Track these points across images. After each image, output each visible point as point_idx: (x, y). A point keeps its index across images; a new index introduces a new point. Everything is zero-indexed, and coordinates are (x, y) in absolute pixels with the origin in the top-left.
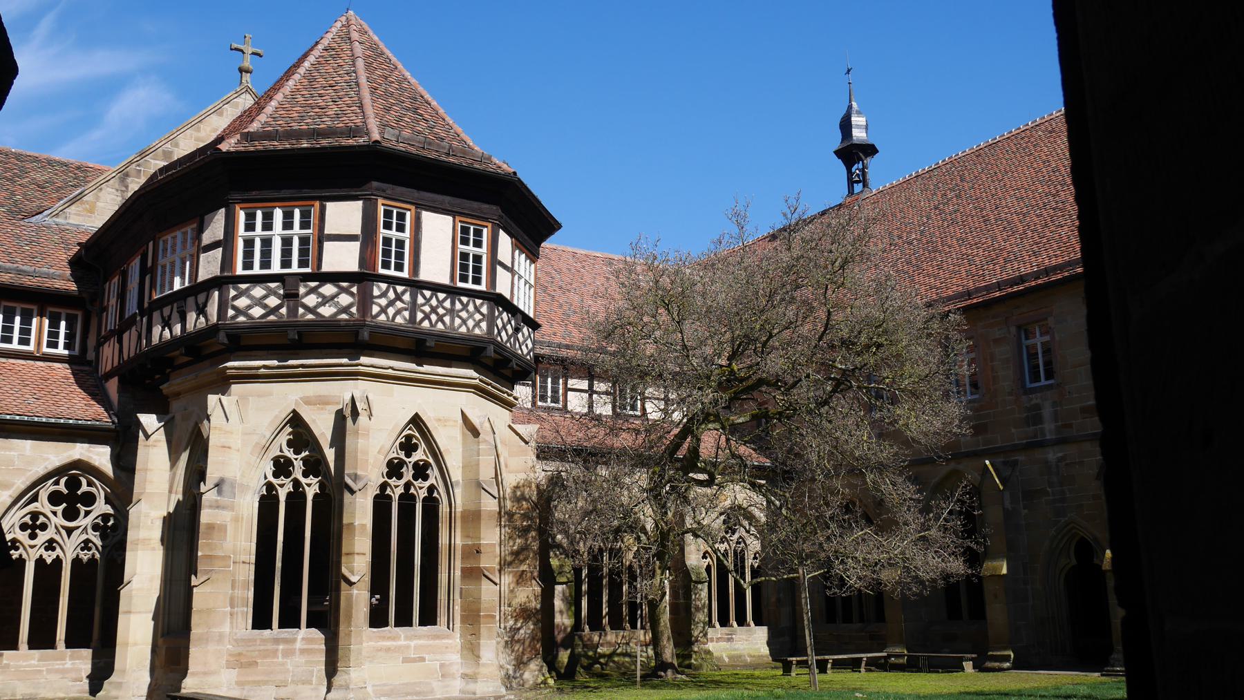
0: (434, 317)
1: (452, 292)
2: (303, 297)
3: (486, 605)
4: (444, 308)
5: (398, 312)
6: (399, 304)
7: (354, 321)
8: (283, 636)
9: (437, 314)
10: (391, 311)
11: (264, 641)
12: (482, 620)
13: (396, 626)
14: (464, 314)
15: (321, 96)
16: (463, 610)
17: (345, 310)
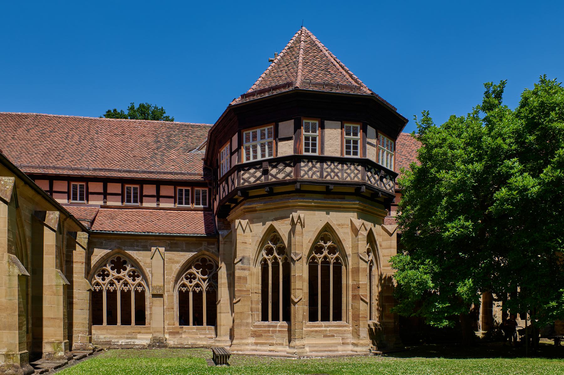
0: (332, 174)
1: (342, 161)
2: (271, 170)
3: (362, 312)
4: (337, 169)
5: (314, 173)
6: (314, 169)
7: (292, 180)
8: (273, 324)
9: (334, 172)
10: (310, 173)
11: (265, 326)
12: (360, 319)
13: (321, 321)
14: (349, 171)
15: (281, 71)
16: (353, 315)
17: (289, 175)
